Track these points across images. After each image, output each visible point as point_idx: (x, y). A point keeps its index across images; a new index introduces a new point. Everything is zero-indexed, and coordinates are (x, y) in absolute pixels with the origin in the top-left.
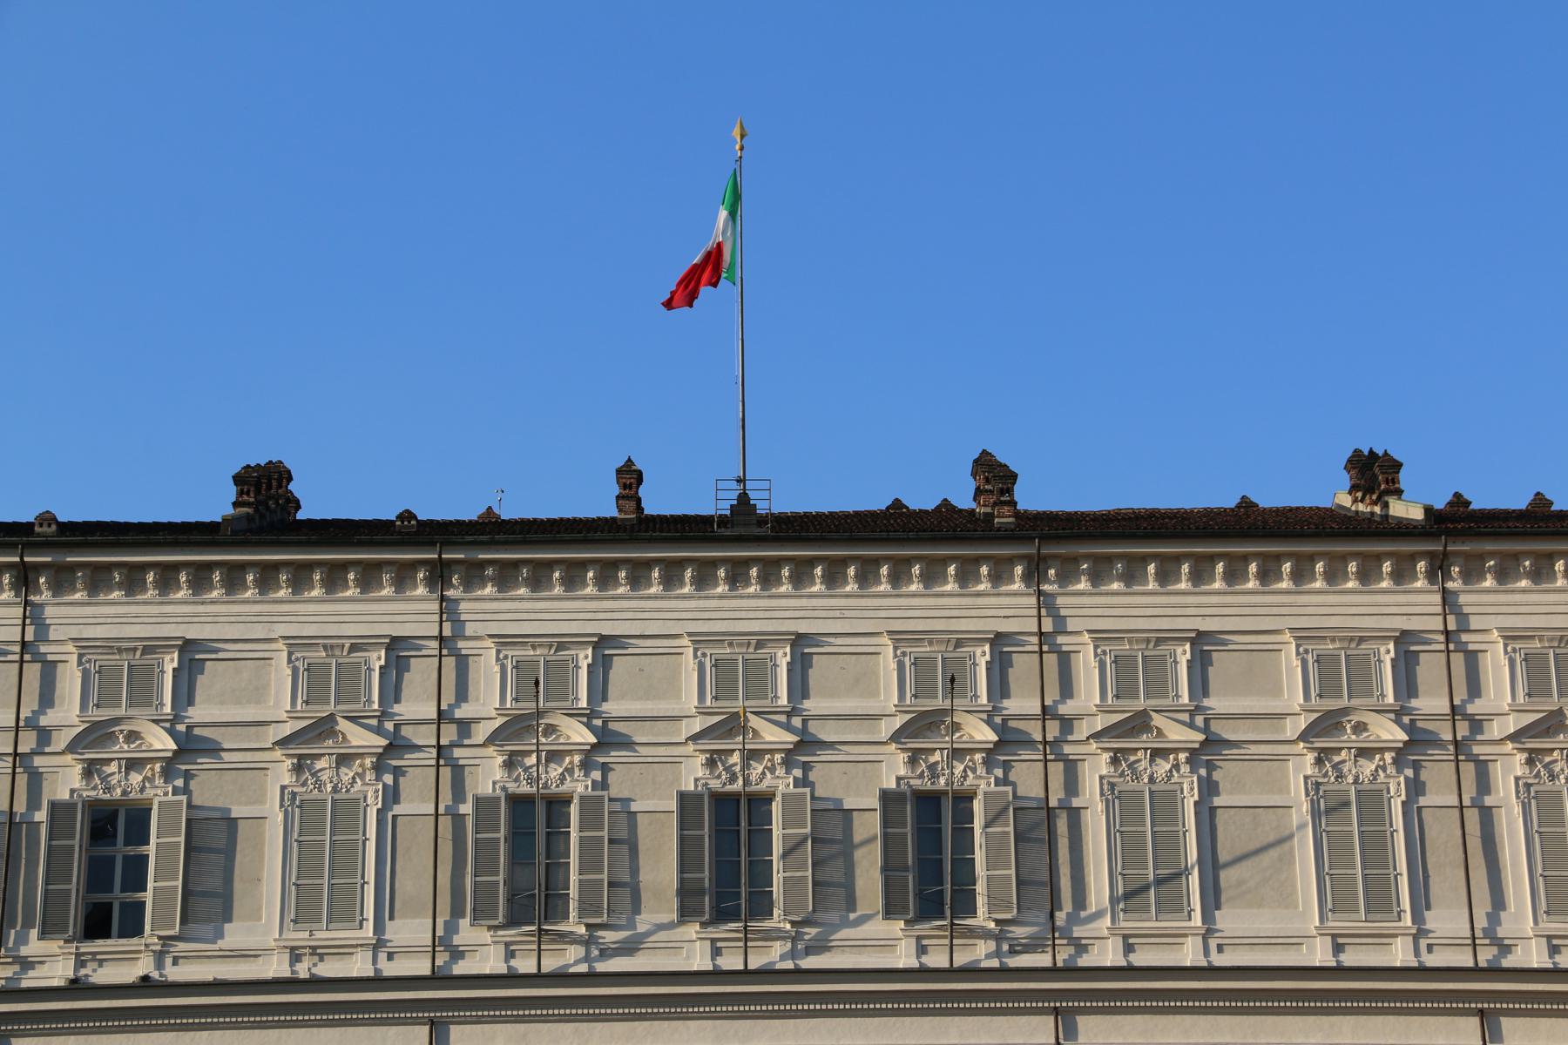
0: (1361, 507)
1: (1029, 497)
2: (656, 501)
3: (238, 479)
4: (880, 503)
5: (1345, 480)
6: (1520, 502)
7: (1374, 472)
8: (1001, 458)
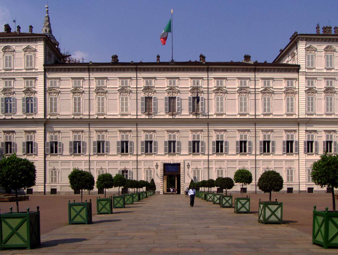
0: (245, 62)
1: (207, 60)
2: (162, 60)
3: (112, 57)
4: (188, 61)
5: (244, 59)
6: (263, 62)
7: (247, 58)
8: (203, 55)
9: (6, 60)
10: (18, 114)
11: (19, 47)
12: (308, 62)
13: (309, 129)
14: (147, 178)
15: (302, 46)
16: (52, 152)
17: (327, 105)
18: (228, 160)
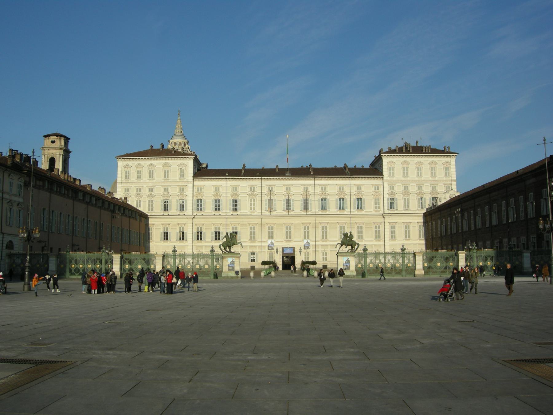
9: (165, 173)
10: (172, 211)
11: (174, 163)
12: (390, 173)
13: (390, 221)
14: (270, 258)
15: (386, 160)
16: (198, 239)
17: (405, 204)
18: (330, 245)
